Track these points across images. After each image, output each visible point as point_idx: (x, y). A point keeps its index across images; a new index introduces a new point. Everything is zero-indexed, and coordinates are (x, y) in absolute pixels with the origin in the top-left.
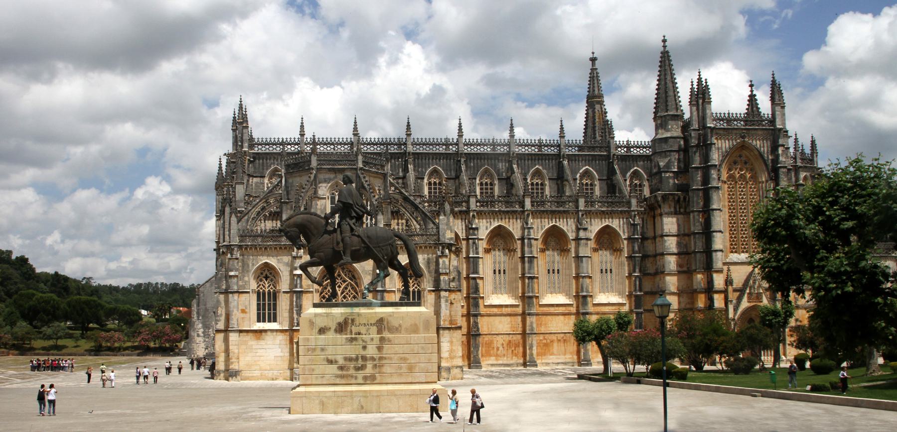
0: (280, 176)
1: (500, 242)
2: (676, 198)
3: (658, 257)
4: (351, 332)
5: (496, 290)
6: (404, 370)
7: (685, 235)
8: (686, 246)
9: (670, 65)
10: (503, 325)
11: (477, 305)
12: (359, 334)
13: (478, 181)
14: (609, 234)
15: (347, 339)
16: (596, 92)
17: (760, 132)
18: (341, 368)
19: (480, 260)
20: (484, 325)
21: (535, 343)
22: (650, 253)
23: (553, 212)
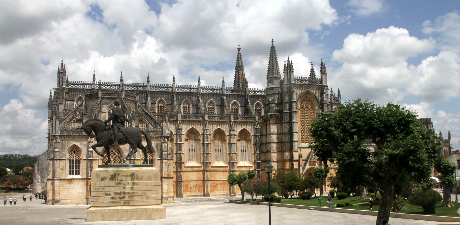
0: (82, 101)
1: (193, 136)
2: (277, 116)
3: (268, 144)
4: (118, 180)
5: (190, 159)
6: (144, 199)
7: (280, 134)
8: (281, 139)
9: (275, 53)
10: (194, 176)
11: (181, 167)
12: (122, 181)
13: (182, 106)
14: (245, 133)
15: (115, 183)
16: (240, 64)
17: (315, 87)
18: (113, 198)
19: (183, 145)
20: (184, 176)
21: (209, 185)
22: (264, 142)
23: (218, 122)
